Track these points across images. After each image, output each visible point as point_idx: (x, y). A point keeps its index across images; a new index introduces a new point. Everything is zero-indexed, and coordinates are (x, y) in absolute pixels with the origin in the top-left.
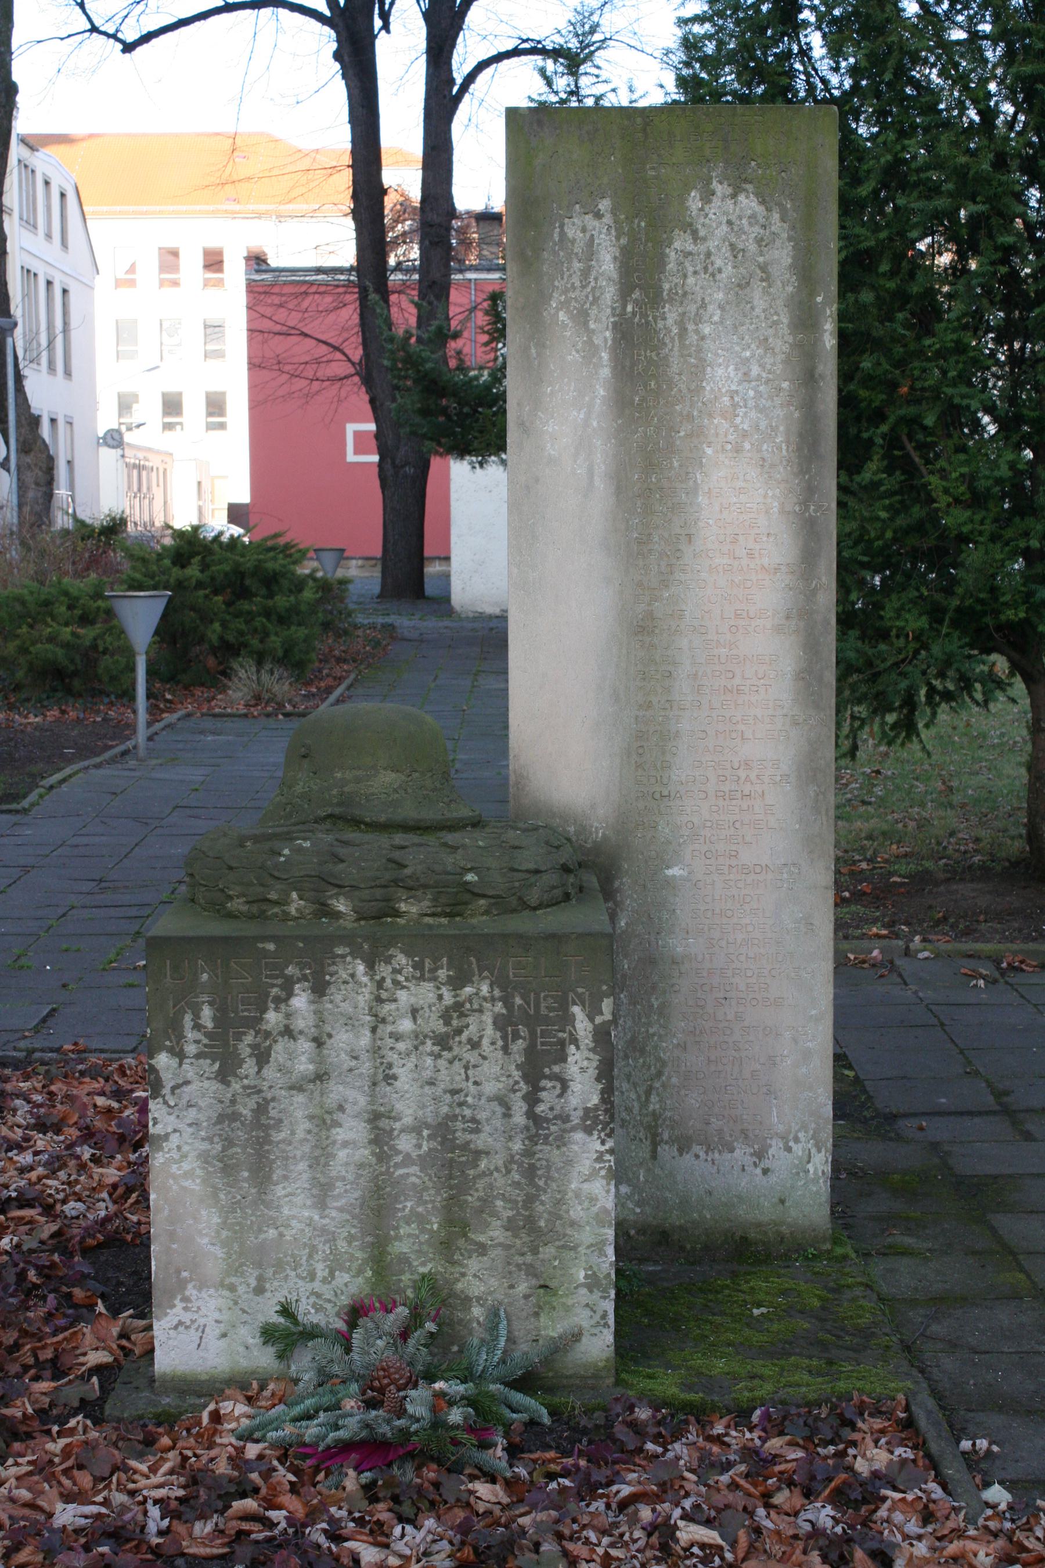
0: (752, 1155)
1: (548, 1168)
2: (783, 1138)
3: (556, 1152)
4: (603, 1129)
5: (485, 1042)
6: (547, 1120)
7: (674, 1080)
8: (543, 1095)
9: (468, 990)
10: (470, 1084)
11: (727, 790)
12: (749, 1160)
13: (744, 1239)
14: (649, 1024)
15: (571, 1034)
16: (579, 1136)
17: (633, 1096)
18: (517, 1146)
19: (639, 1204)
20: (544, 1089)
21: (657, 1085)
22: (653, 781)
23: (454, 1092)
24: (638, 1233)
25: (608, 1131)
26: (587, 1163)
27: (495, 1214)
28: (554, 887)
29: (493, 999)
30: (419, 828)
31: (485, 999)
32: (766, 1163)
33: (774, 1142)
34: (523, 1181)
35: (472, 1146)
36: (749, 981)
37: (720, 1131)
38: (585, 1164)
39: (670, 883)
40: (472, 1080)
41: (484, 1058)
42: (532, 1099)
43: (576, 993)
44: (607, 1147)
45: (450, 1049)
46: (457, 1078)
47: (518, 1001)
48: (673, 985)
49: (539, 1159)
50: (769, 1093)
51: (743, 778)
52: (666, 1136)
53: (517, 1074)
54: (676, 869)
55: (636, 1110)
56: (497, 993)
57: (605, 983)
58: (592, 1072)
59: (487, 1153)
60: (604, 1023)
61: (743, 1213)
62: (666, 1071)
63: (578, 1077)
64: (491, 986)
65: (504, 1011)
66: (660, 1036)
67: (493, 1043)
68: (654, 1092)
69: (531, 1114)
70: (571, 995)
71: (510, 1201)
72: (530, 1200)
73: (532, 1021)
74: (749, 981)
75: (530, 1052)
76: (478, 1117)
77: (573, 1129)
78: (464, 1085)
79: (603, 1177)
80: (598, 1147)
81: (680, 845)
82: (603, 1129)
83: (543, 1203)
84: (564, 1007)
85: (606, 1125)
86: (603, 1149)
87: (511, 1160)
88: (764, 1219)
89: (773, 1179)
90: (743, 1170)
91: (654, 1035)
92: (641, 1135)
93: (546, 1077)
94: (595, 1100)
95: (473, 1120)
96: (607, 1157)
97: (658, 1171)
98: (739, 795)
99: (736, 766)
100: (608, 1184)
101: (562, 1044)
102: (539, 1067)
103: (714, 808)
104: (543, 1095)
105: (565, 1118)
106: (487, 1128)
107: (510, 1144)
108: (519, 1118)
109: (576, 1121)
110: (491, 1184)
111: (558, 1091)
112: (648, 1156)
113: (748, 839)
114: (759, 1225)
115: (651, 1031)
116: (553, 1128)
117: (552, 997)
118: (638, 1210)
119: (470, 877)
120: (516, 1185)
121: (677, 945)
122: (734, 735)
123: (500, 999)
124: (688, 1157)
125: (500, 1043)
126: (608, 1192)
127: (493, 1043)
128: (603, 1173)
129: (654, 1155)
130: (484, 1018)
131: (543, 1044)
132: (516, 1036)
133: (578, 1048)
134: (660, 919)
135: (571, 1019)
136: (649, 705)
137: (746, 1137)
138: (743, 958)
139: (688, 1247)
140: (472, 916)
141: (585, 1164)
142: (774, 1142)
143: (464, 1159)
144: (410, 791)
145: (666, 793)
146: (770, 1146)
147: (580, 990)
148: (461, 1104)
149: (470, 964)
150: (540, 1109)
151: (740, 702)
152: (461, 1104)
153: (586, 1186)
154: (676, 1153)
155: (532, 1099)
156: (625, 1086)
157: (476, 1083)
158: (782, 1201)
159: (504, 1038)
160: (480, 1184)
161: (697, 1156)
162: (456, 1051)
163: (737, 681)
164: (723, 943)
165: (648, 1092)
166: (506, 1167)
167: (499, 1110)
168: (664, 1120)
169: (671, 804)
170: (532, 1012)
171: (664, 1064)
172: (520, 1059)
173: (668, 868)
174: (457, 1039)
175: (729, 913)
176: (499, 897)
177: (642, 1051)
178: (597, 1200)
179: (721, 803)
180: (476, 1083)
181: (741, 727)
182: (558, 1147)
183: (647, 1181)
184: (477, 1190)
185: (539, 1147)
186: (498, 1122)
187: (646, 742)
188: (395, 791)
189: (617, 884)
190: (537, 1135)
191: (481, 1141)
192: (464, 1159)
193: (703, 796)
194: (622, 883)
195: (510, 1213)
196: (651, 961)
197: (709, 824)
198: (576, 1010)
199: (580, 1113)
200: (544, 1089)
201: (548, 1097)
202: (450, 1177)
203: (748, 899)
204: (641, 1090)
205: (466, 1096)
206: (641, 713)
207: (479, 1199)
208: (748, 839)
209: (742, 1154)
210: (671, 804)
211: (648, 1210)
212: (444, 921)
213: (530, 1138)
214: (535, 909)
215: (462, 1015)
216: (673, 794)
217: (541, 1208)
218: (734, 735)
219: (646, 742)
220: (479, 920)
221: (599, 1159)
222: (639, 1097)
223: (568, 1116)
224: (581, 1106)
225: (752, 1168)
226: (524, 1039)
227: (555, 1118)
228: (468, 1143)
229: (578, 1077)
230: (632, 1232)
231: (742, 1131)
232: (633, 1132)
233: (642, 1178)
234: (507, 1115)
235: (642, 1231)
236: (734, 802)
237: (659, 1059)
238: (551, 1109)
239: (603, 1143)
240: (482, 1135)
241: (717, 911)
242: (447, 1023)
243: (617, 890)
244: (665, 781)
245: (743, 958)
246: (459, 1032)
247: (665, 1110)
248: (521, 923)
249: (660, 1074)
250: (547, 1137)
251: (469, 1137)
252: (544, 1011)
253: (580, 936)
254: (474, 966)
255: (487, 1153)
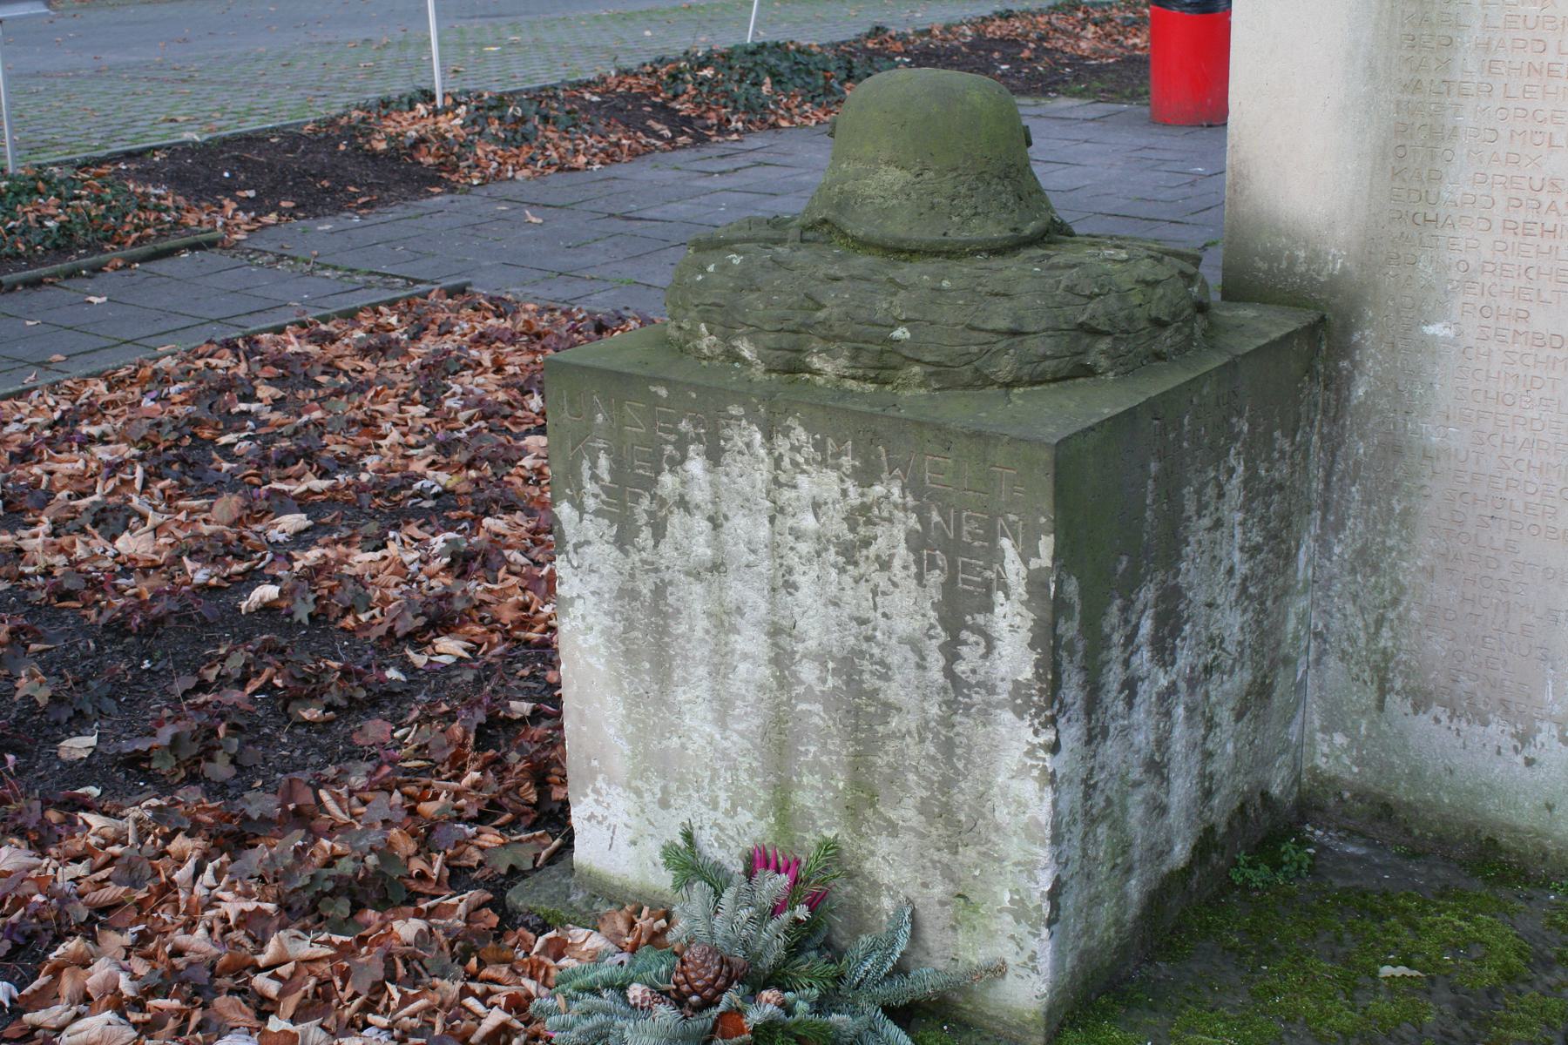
0: (1513, 736)
1: (969, 748)
2: (1559, 724)
3: (981, 730)
4: (1037, 715)
5: (897, 563)
6: (970, 686)
7: (1415, 614)
8: (964, 650)
9: (878, 489)
10: (879, 615)
11: (1520, 220)
12: (1508, 742)
13: (1492, 841)
14: (1387, 533)
15: (999, 577)
16: (1007, 716)
17: (1360, 624)
18: (934, 711)
19: (1359, 761)
20: (965, 643)
21: (1391, 615)
22: (1414, 196)
23: (863, 622)
24: (1354, 796)
25: (1043, 719)
26: (1018, 754)
27: (905, 787)
28: (1045, 357)
29: (905, 508)
30: (902, 251)
31: (896, 506)
32: (1530, 752)
33: (1545, 726)
34: (939, 756)
35: (881, 696)
36: (1531, 499)
37: (1471, 696)
38: (1013, 756)
39: (1429, 346)
40: (880, 611)
41: (895, 585)
42: (951, 653)
43: (1006, 520)
44: (1042, 739)
45: (856, 564)
46: (864, 604)
47: (935, 517)
48: (1423, 487)
49: (958, 734)
50: (1545, 659)
51: (1545, 206)
52: (1398, 685)
53: (933, 615)
54: (1440, 325)
55: (1362, 642)
56: (910, 500)
57: (1043, 514)
58: (1025, 635)
59: (899, 710)
60: (1040, 569)
61: (1493, 808)
62: (1405, 600)
63: (1006, 634)
64: (903, 489)
65: (918, 527)
66: (1400, 552)
67: (905, 568)
68: (1387, 624)
69: (949, 672)
70: (1001, 521)
71: (923, 778)
72: (947, 784)
73: (954, 548)
74: (1531, 499)
75: (949, 586)
76: (889, 660)
77: (1000, 705)
78: (871, 614)
79: (1035, 778)
80: (1028, 735)
81: (1446, 293)
82: (1037, 715)
83: (961, 791)
84: (991, 536)
85: (1041, 710)
86: (1036, 741)
87: (924, 726)
88: (1524, 823)
89: (1539, 774)
90: (1499, 753)
91: (1391, 549)
92: (1366, 676)
93: (967, 627)
94: (1028, 673)
95: (882, 663)
96: (1041, 753)
97: (1384, 726)
98: (1537, 230)
99: (1537, 185)
100: (1042, 790)
101: (988, 586)
102: (960, 611)
103: (1501, 246)
104: (964, 650)
105: (991, 690)
106: (898, 677)
107: (926, 705)
108: (936, 674)
109: (1006, 696)
110: (902, 750)
111: (982, 650)
112: (1373, 704)
113: (1546, 296)
114: (1515, 829)
115: (1389, 543)
116: (976, 698)
117: (976, 519)
118: (1355, 770)
119: (901, 333)
120: (932, 759)
121: (1433, 433)
122: (1538, 139)
123: (914, 510)
124: (1424, 720)
125: (913, 569)
126: (1041, 799)
127: (905, 568)
128: (1036, 773)
129: (1381, 707)
130: (895, 531)
131: (965, 581)
132: (933, 565)
133: (1007, 597)
134: (1411, 393)
135: (1000, 556)
136: (1417, 86)
137: (1507, 711)
138: (1523, 466)
139: (1417, 832)
140: (905, 386)
141: (1013, 756)
142: (1545, 726)
143: (872, 709)
144: (914, 196)
145: (1431, 216)
146: (1540, 730)
147: (1012, 517)
148: (868, 639)
149: (879, 457)
150: (961, 668)
151: (1551, 89)
152: (868, 639)
153: (1015, 784)
154: (1410, 710)
155: (951, 653)
156: (1350, 608)
157: (885, 615)
158: (1550, 808)
159: (918, 562)
160: (891, 746)
161: (1437, 720)
162: (863, 568)
163: (1550, 57)
164: (1497, 440)
165: (1379, 623)
166: (920, 734)
167: (913, 658)
168: (1398, 664)
169: (1438, 232)
170: (951, 536)
171: (1402, 590)
172: (938, 597)
173: (1427, 323)
174: (865, 552)
175: (1509, 400)
176: (938, 364)
177: (1375, 569)
178: (1027, 806)
179: (1510, 238)
180: (885, 615)
181: (1549, 127)
182: (984, 725)
183: (1368, 736)
184: (886, 753)
185: (958, 718)
186: (912, 673)
187: (1410, 141)
188: (895, 195)
189: (1356, 337)
190: (955, 701)
191: (893, 691)
192: (872, 709)
193: (1484, 225)
194: (1363, 337)
195: (925, 794)
196: (1394, 449)
197: (1491, 268)
198: (1006, 543)
199: (1009, 686)
200: (965, 643)
201: (970, 654)
202: (857, 728)
203: (1538, 384)
204: (1371, 619)
205: (875, 629)
206: (1406, 97)
207: (889, 765)
208: (1546, 296)
209: (1498, 731)
210: (1438, 232)
211: (1368, 772)
212: (871, 387)
213: (948, 703)
214: (1008, 385)
215: (869, 522)
216: (1441, 220)
217: (961, 798)
218: (1538, 139)
219: (1410, 141)
220: (912, 393)
221: (1031, 753)
222: (1366, 626)
223: (994, 687)
224: (1010, 677)
225: (1511, 753)
226: (942, 570)
227: (979, 684)
228: (876, 691)
229: (1006, 634)
230: (1347, 795)
231: (1502, 702)
232: (1355, 670)
233: (1363, 731)
234: (921, 667)
235: (1359, 796)
236: (1529, 239)
237: (1395, 582)
238: (974, 671)
239: (1036, 733)
240: (894, 685)
241: (1492, 394)
242: (852, 529)
243: (1357, 346)
244: (1432, 199)
245: (1523, 466)
246: (866, 543)
247: (1399, 650)
248: (959, 410)
249: (1395, 602)
250: (968, 707)
251: (879, 683)
252: (966, 538)
253: (1013, 440)
254: (884, 458)
255: (899, 710)
